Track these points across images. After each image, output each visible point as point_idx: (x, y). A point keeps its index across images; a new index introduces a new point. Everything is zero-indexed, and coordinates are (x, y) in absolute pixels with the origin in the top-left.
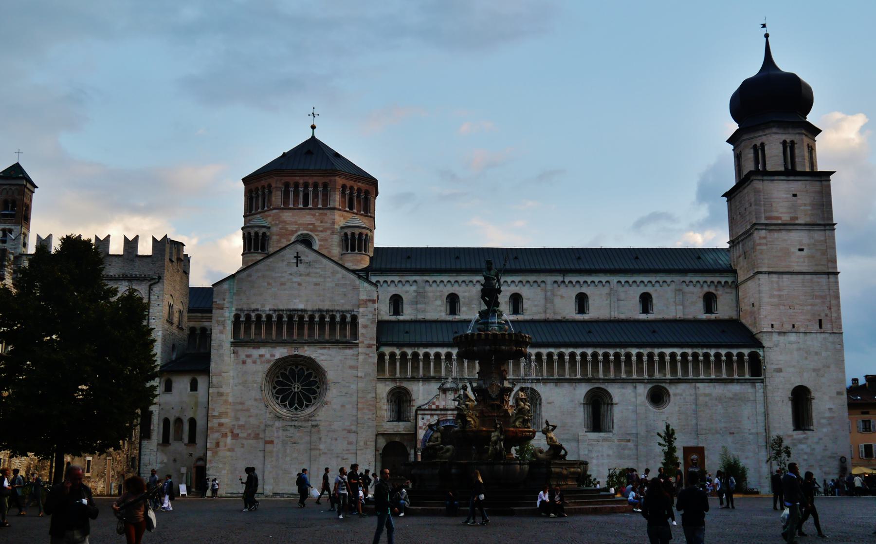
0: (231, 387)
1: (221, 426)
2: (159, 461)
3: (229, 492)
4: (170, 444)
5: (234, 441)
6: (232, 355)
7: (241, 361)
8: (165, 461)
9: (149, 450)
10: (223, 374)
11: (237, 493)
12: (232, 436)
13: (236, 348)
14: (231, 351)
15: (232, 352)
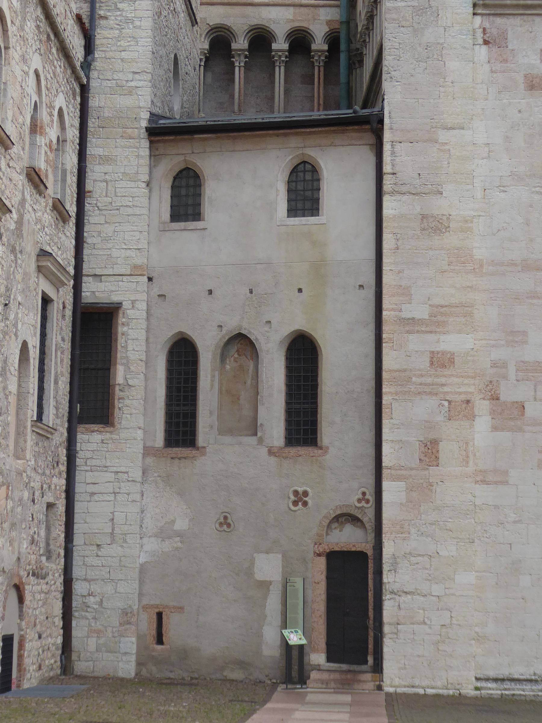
0: (479, 194)
1: (444, 366)
2: (150, 524)
3: (492, 674)
4: (202, 450)
5: (504, 436)
6: (483, 51)
7: (520, 79)
8: (181, 524)
9: (110, 476)
10: (443, 136)
11: (530, 681)
12: (493, 412)
13: (499, 21)
14: (474, 31)
15: (481, 41)
